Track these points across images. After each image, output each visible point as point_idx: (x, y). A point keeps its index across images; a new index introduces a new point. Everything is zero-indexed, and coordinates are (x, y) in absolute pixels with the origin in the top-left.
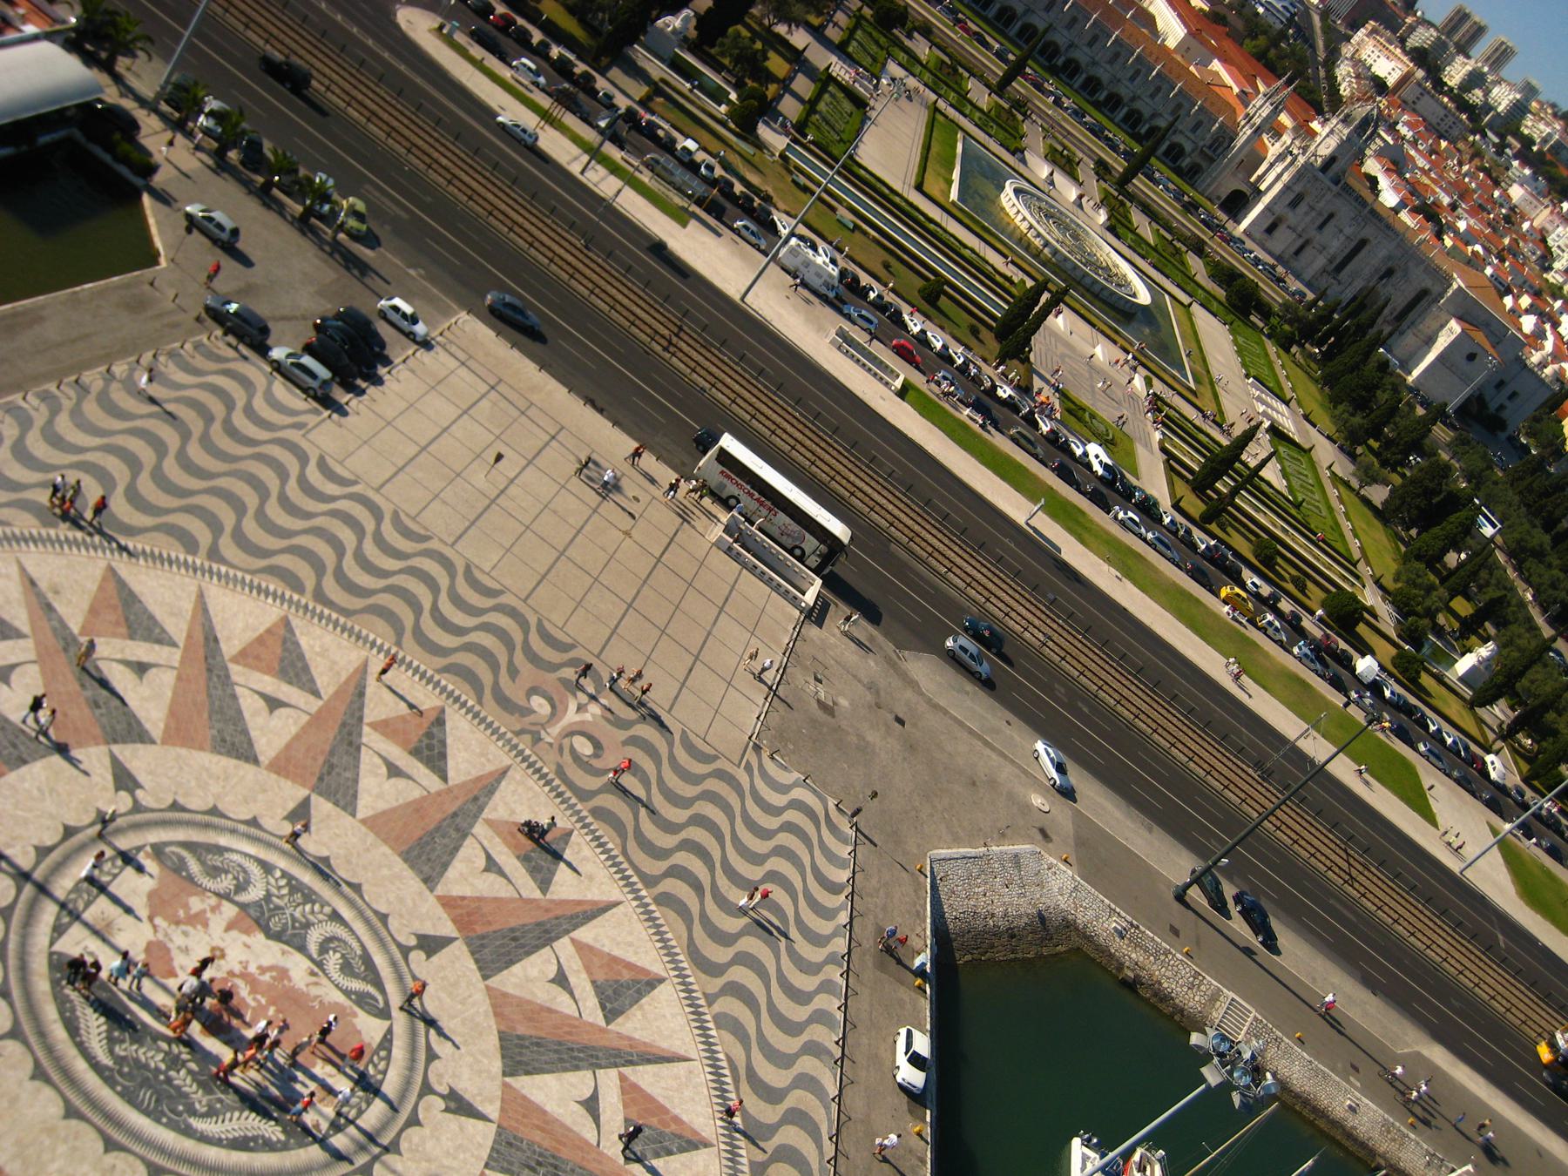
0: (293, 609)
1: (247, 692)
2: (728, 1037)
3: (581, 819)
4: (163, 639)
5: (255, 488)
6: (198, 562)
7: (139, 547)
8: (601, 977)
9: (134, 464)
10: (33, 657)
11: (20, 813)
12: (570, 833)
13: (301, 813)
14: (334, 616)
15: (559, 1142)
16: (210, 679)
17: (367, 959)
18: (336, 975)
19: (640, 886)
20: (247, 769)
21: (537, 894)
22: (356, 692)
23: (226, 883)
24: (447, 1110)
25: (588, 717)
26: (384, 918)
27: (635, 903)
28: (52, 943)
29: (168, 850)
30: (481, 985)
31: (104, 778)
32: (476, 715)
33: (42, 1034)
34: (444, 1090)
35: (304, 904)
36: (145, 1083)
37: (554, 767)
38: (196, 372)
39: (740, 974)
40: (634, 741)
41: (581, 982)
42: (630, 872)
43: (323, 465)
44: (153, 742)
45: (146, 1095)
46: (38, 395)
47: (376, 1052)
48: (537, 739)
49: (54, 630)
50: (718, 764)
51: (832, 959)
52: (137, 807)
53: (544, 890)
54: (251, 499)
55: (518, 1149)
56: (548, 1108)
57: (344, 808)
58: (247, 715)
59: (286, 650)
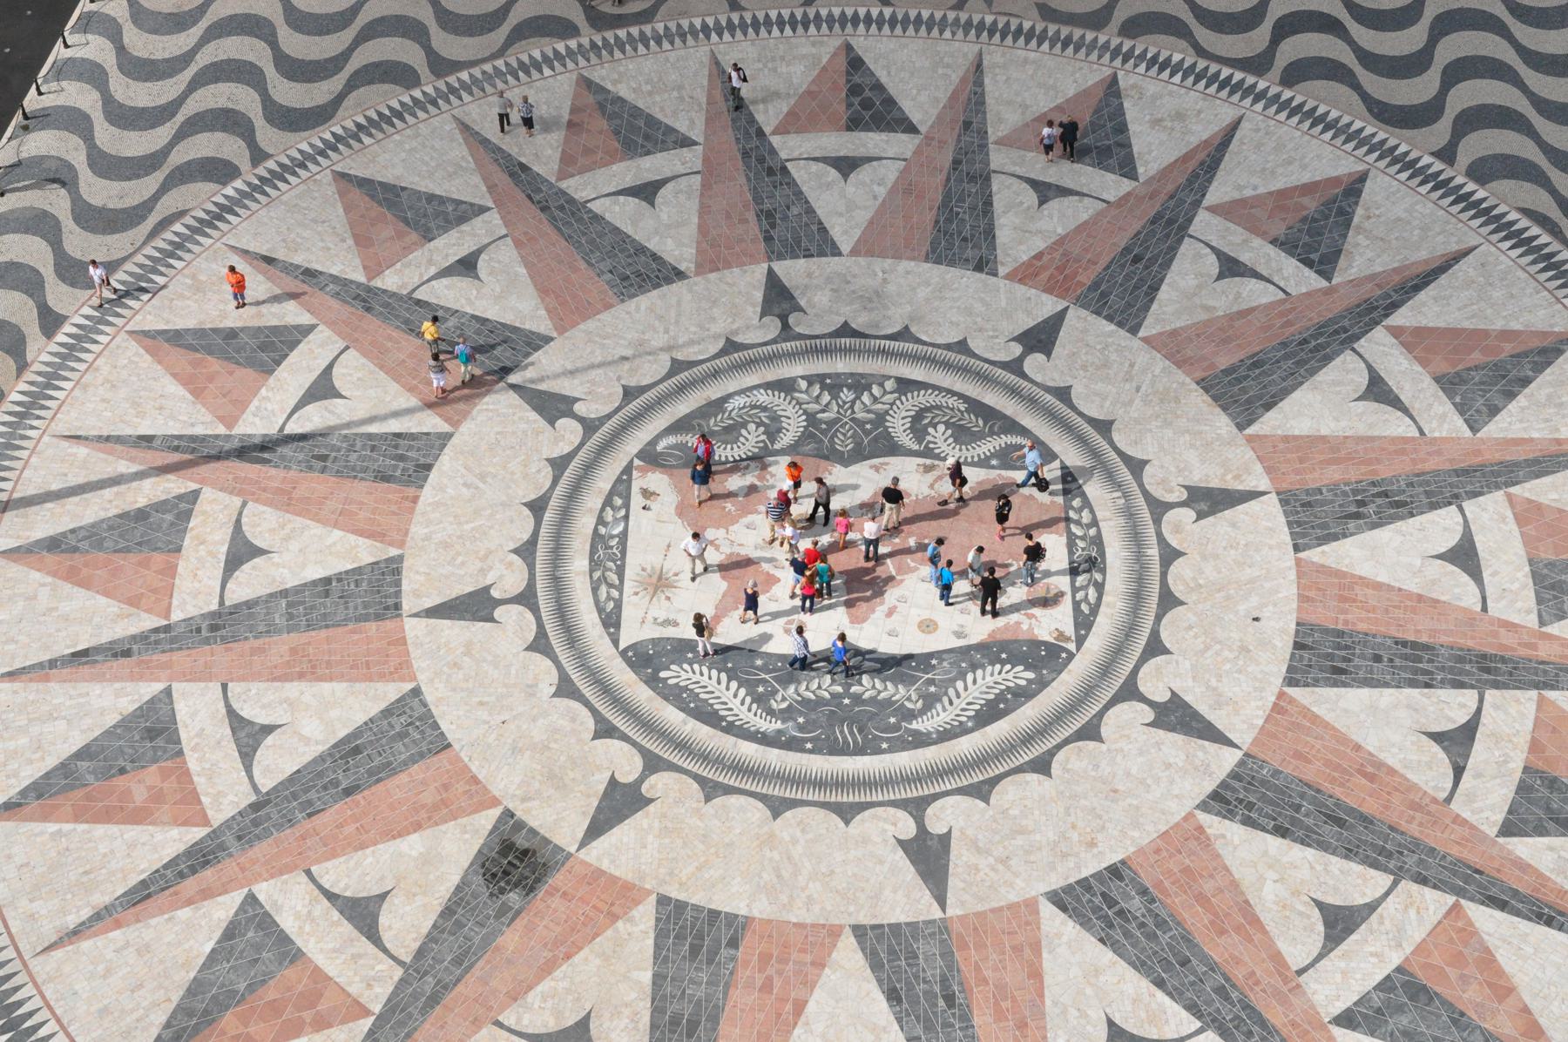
0: (582, 62)
1: (607, 201)
2: (1504, 186)
3: (1116, 53)
4: (463, 213)
6: (429, 89)
7: (350, 124)
8: (1279, 229)
10: (341, 345)
11: (467, 527)
12: (1114, 80)
14: (635, 31)
15: (1369, 462)
16: (553, 220)
17: (976, 407)
19: (1250, 80)
20: (677, 287)
21: (1127, 185)
24: (1201, 516)
26: (962, 347)
27: (1259, 107)
28: (616, 642)
29: (660, 447)
30: (1136, 343)
33: (682, 746)
35: (858, 397)
36: (834, 719)
37: (1035, 13)
41: (1257, 251)
44: (548, 340)
45: (844, 733)
49: (337, 295)
52: (590, 426)
53: (1136, 179)
55: (1323, 503)
56: (1324, 431)
57: (822, 254)
58: (628, 229)
59: (610, 118)
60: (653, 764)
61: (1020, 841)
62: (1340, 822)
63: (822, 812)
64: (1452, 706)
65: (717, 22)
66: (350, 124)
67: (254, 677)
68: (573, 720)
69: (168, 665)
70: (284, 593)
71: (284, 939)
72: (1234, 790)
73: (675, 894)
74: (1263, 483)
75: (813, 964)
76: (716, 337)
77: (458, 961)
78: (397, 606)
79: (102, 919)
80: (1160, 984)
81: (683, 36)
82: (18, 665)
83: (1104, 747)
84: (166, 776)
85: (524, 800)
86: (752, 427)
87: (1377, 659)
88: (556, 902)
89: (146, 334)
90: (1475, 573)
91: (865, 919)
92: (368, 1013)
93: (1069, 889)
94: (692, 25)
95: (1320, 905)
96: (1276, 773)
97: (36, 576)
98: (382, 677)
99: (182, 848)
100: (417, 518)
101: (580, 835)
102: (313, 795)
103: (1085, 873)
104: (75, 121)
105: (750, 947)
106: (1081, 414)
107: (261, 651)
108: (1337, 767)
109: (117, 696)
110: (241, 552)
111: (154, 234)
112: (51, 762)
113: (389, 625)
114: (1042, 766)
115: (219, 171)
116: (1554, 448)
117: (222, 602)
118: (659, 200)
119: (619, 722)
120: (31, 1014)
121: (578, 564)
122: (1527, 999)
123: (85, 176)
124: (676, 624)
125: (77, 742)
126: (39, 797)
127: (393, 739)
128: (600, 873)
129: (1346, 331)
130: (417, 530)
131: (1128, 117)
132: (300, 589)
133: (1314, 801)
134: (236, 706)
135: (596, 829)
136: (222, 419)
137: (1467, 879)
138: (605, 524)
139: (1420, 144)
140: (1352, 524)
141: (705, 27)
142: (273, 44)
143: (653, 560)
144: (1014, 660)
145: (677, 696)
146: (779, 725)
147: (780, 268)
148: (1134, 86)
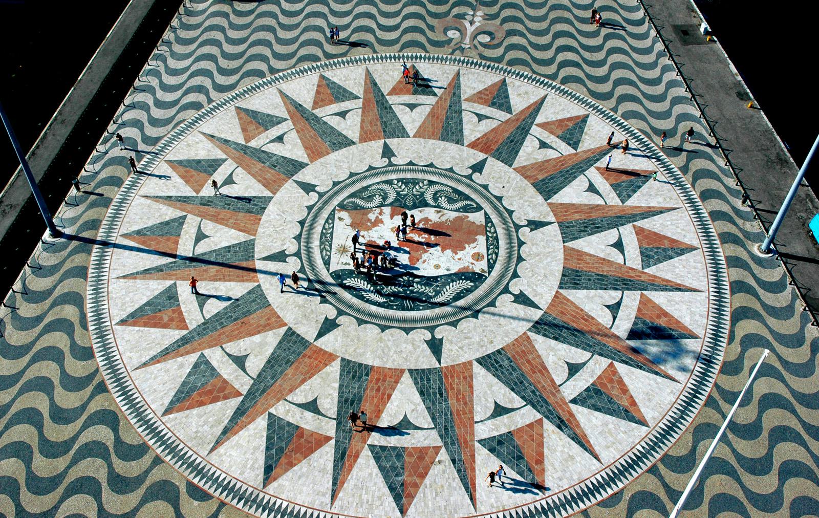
1: (328, 117)
2: (633, 121)
4: (280, 121)
5: (267, 31)
6: (269, 79)
7: (241, 90)
8: (560, 133)
9: (211, 58)
12: (504, 80)
13: (387, 152)
14: (340, 60)
15: (588, 213)
17: (456, 191)
19: (550, 82)
20: (353, 147)
21: (509, 116)
22: (372, 84)
23: (377, 200)
24: (532, 230)
25: (477, 24)
26: (451, 170)
27: (553, 91)
28: (328, 271)
30: (511, 170)
31: (299, 193)
33: (350, 306)
37: (478, 57)
39: (621, 90)
40: (505, 20)
41: (551, 139)
42: (542, 79)
45: (407, 303)
46: (152, 59)
47: (486, 226)
48: (462, 50)
51: (660, 55)
52: (321, 195)
53: (510, 113)
54: (269, 36)
55: (573, 227)
56: (574, 202)
60: (340, 313)
61: (467, 341)
62: (575, 336)
63: (399, 331)
64: (612, 296)
65: (368, 57)
66: (241, 90)
67: (205, 279)
69: (176, 275)
70: (215, 251)
71: (213, 369)
73: (347, 357)
76: (365, 164)
77: (272, 378)
78: (253, 256)
79: (155, 360)
80: (513, 390)
81: (357, 62)
82: (126, 274)
84: (174, 311)
86: (377, 196)
87: (590, 280)
88: (306, 360)
90: (622, 252)
91: (413, 368)
92: (241, 395)
93: (483, 358)
94: (360, 58)
95: (567, 363)
96: (555, 319)
99: (179, 337)
101: (315, 337)
103: (489, 352)
104: (150, 90)
105: (373, 376)
106: (491, 194)
107: (206, 271)
108: (575, 317)
110: (200, 236)
111: (174, 128)
112: (137, 306)
115: (197, 106)
118: (347, 117)
120: (131, 390)
121: (316, 243)
122: (632, 394)
124: (349, 264)
125: (145, 300)
127: (251, 302)
128: (321, 350)
130: (260, 230)
131: (510, 92)
135: (320, 335)
136: (194, 191)
137: (615, 354)
138: (326, 229)
139: (605, 106)
140: (582, 234)
141: (364, 58)
142: (217, 63)
143: (342, 242)
144: (466, 279)
146: (385, 300)
147: (388, 141)
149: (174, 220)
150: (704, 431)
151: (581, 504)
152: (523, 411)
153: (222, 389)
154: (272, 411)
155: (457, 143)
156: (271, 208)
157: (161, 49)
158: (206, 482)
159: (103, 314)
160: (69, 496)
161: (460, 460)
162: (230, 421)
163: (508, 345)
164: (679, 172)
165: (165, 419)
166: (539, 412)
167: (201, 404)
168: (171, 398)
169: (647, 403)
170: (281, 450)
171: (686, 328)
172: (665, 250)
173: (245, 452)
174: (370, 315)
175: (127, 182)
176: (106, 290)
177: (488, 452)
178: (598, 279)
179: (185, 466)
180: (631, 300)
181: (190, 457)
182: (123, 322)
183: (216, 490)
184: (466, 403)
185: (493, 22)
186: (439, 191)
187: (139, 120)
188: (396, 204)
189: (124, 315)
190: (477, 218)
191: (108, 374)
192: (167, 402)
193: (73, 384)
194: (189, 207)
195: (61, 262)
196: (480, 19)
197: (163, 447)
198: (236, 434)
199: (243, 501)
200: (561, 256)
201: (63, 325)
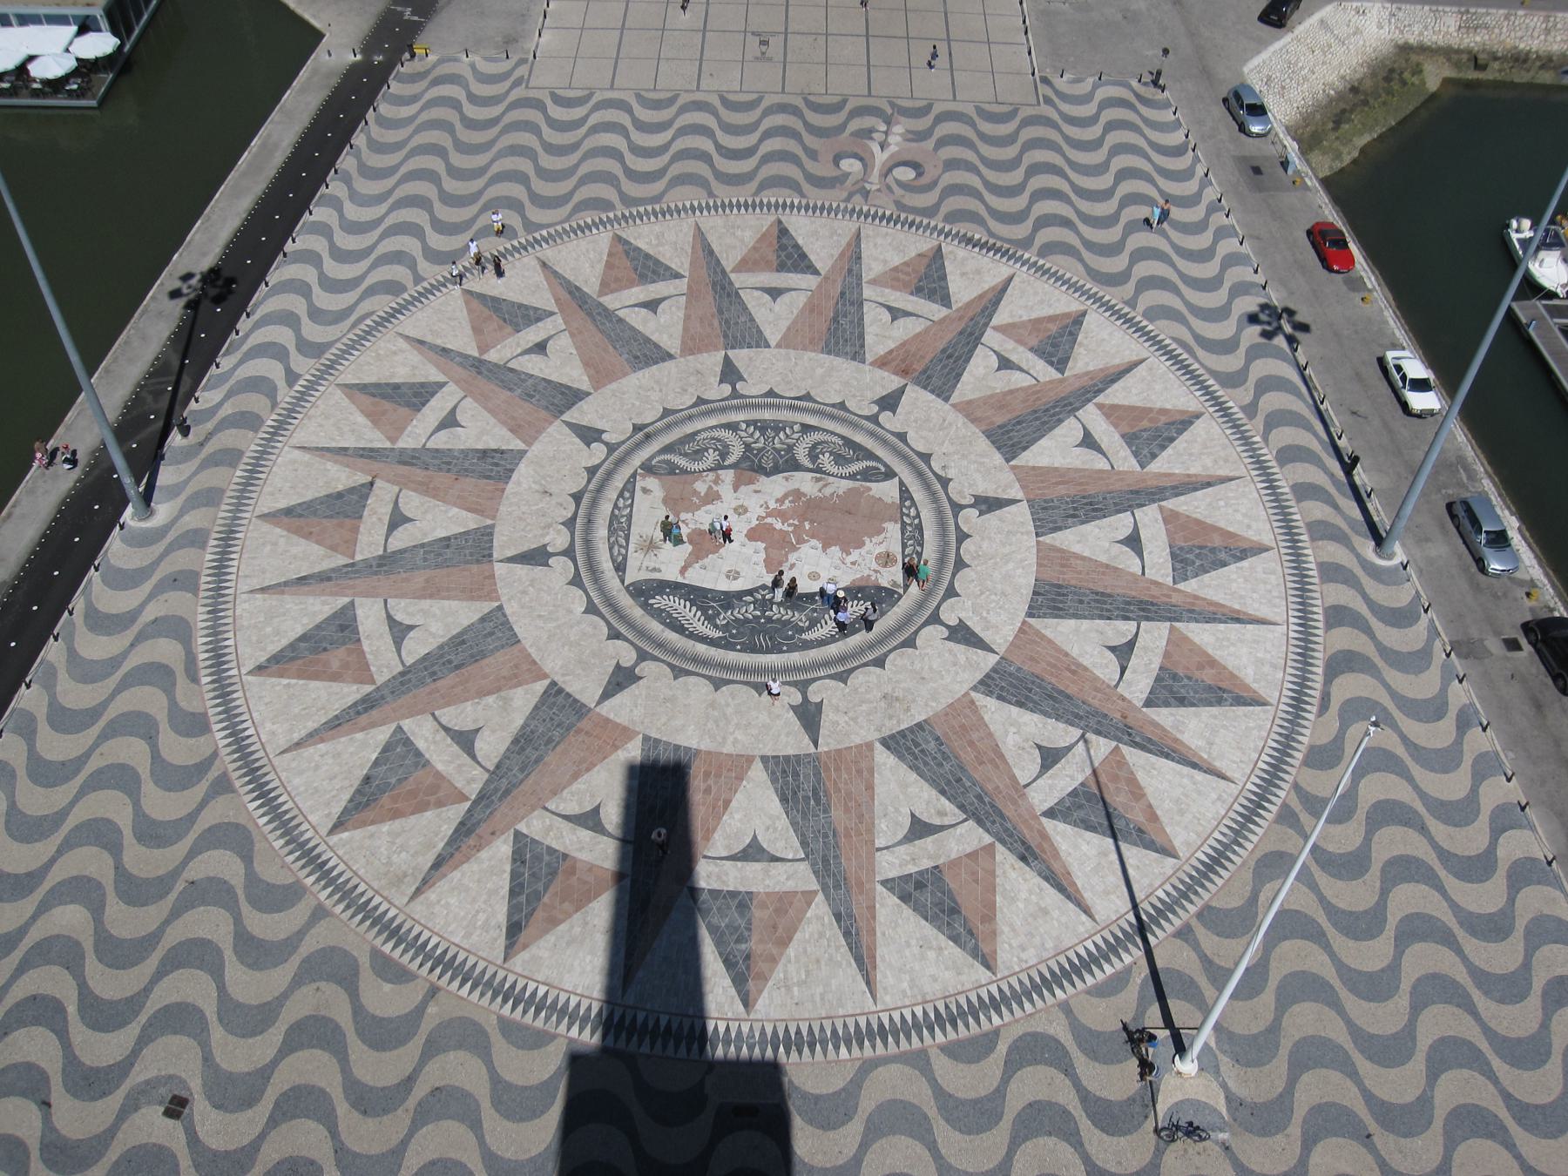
0: (616, 226)
1: (627, 310)
2: (1163, 323)
6: (523, 241)
8: (1034, 342)
10: (463, 394)
11: (534, 508)
12: (940, 247)
13: (730, 373)
14: (649, 208)
15: (1081, 484)
17: (849, 443)
18: (835, 470)
21: (944, 312)
22: (705, 251)
23: (711, 457)
25: (893, 149)
26: (842, 406)
27: (1025, 268)
28: (623, 582)
30: (947, 407)
31: (573, 444)
32: (807, 208)
33: (661, 645)
34: (970, 500)
38: (413, 99)
39: (1144, 269)
40: (942, 142)
41: (1020, 355)
43: (559, 100)
44: (589, 394)
45: (761, 640)
47: (902, 505)
48: (866, 194)
49: (461, 364)
50: (1022, 114)
51: (1213, 208)
52: (611, 448)
54: (525, 165)
55: (1053, 508)
57: (758, 346)
58: (640, 328)
59: (633, 259)
60: (643, 656)
61: (864, 707)
63: (745, 688)
65: (700, 204)
67: (403, 596)
68: (595, 628)
70: (423, 546)
71: (418, 754)
72: (993, 679)
73: (654, 735)
74: (1020, 495)
75: (736, 778)
77: (522, 770)
78: (491, 555)
79: (314, 737)
80: (943, 792)
81: (679, 212)
83: (917, 652)
85: (563, 675)
86: (711, 451)
87: (1081, 602)
88: (581, 737)
89: (346, 386)
90: (1140, 554)
91: (769, 751)
92: (467, 799)
93: (892, 737)
95: (1039, 747)
97: (278, 530)
98: (479, 598)
99: (358, 696)
100: (504, 501)
101: (597, 698)
102: (436, 668)
103: (903, 727)
104: (312, 258)
106: (913, 450)
108: (1054, 666)
109: (324, 603)
110: (398, 520)
111: (354, 326)
112: (284, 642)
113: (485, 566)
114: (880, 663)
115: (394, 288)
116: (1187, 479)
117: (385, 550)
119: (623, 630)
121: (601, 532)
123: (316, 289)
125: (299, 631)
126: (278, 663)
127: (486, 636)
128: (607, 720)
129: (1071, 404)
132: (430, 544)
133: (1040, 686)
134: (392, 613)
135: (606, 695)
138: (619, 509)
140: (1070, 520)
141: (692, 207)
145: (658, 614)
147: (731, 353)
148: (951, 252)
149: (352, 490)
150: (1273, 865)
151: (1058, 992)
152: (960, 830)
153: (434, 789)
154: (522, 827)
155: (854, 358)
156: (523, 472)
157: (334, 187)
158: (405, 951)
159: (225, 655)
160: (167, 973)
161: (850, 916)
162: (448, 844)
163: (936, 715)
164: (1240, 415)
165: (334, 839)
166: (988, 831)
167: (396, 814)
168: (343, 804)
169: (1177, 818)
170: (537, 896)
171: (1247, 688)
172: (1213, 550)
173: (474, 900)
174: (696, 659)
175: (270, 423)
176: (230, 613)
177: (898, 901)
178: (1097, 601)
179: (368, 923)
180: (1154, 637)
181: (376, 908)
182: (260, 669)
183: (421, 965)
184: (861, 817)
185: (923, 144)
186: (819, 443)
187: (292, 313)
188: (744, 465)
189: (263, 658)
190: (887, 491)
191: (234, 761)
192: (337, 810)
193: (174, 778)
194: (375, 466)
195: (153, 563)
196: (898, 139)
197: (330, 889)
198: (456, 867)
199: (469, 984)
200: (1032, 558)
201: (158, 674)
